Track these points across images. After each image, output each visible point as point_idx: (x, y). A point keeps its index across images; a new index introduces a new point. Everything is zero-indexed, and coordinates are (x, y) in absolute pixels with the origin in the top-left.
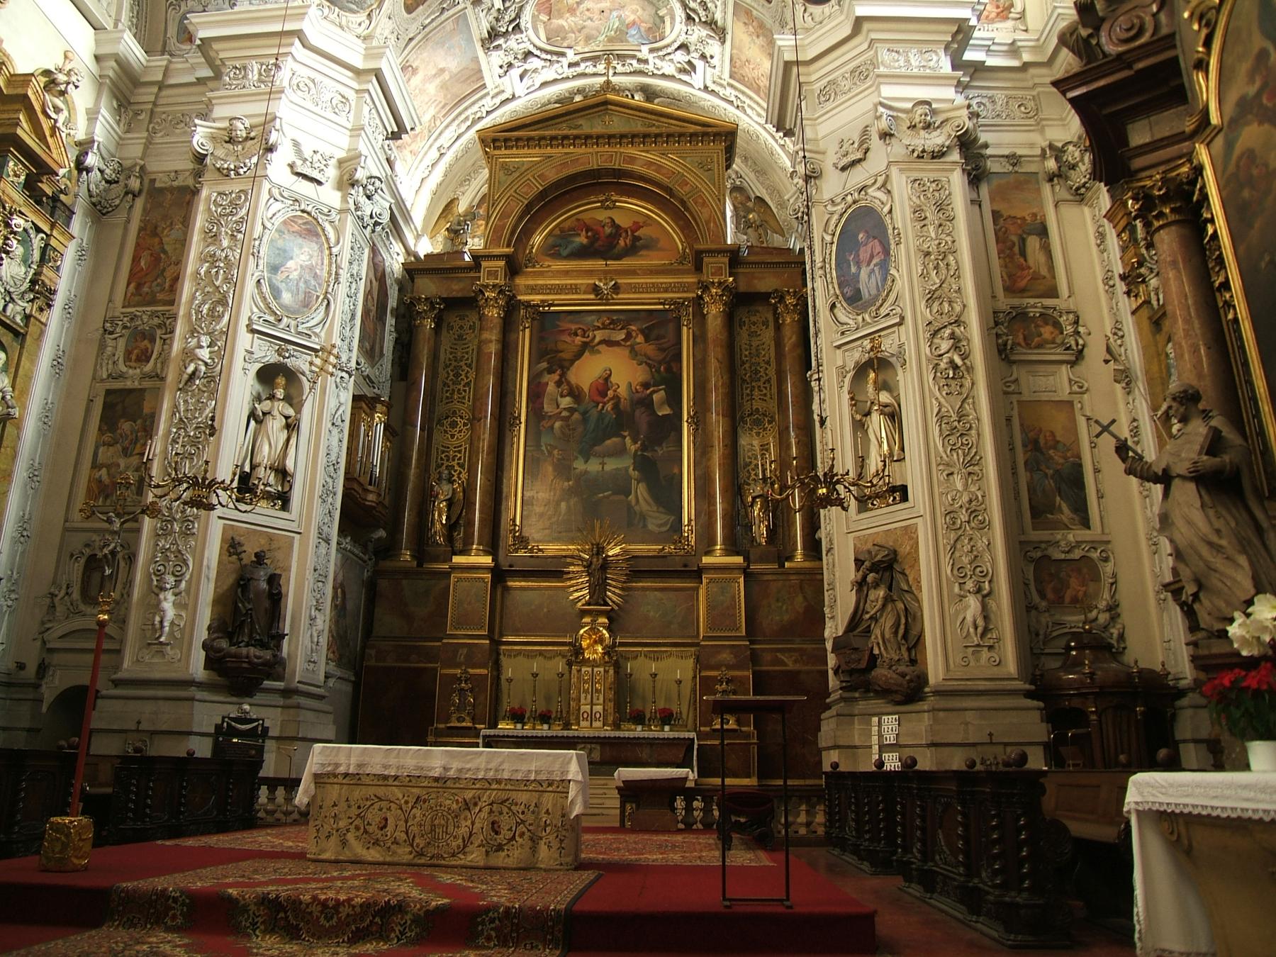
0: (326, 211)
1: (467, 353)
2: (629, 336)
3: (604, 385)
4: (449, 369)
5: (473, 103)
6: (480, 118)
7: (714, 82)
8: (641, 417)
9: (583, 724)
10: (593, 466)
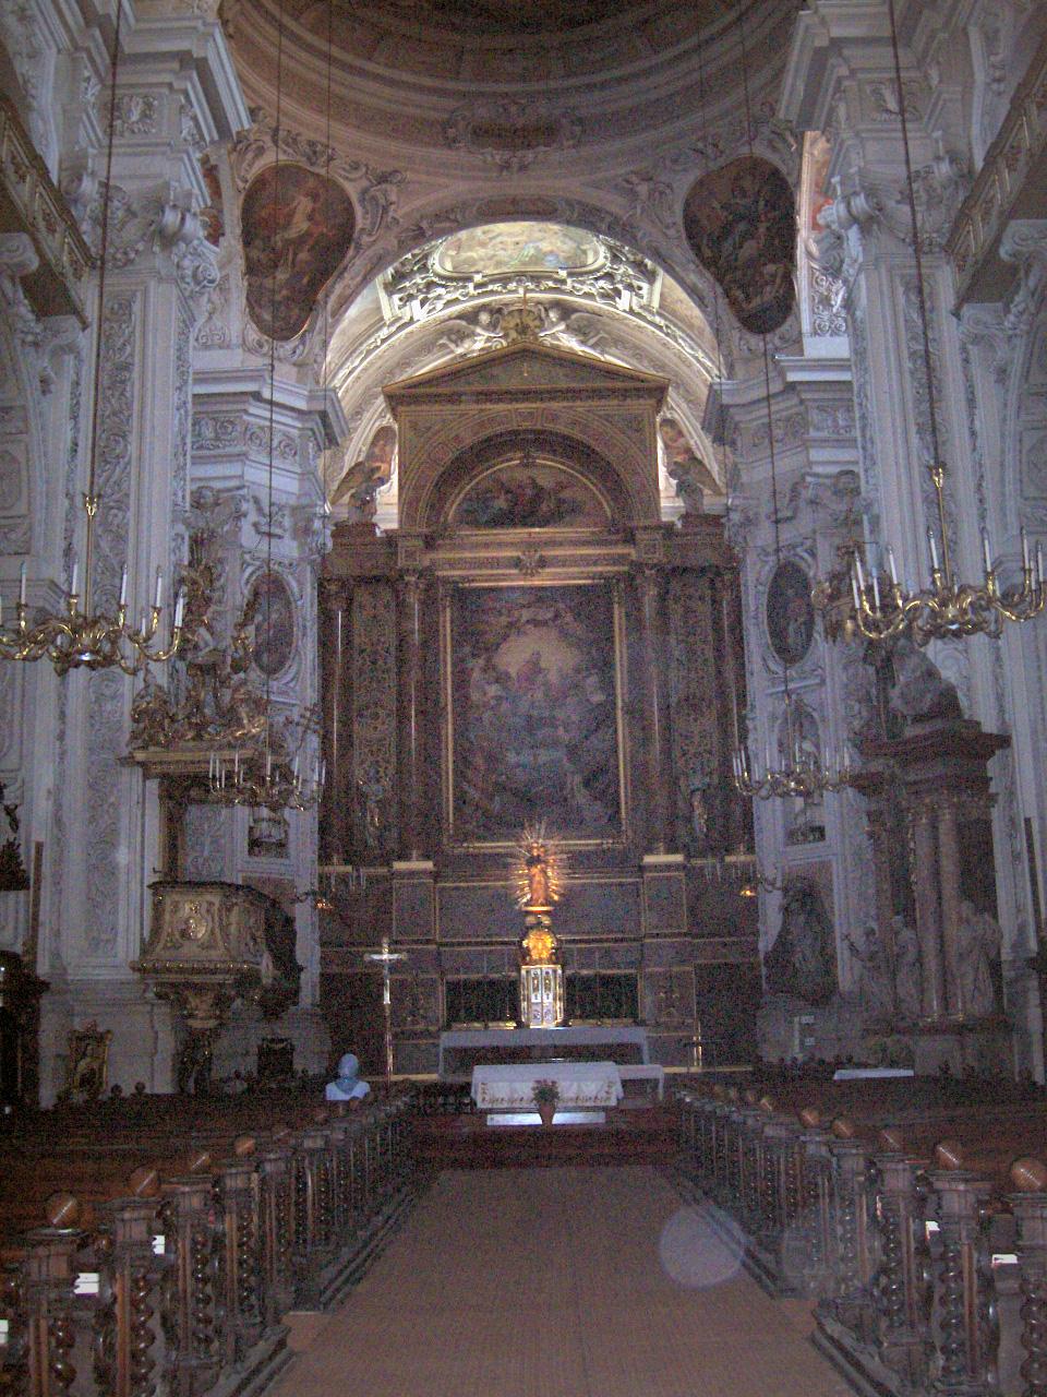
2: (557, 616)
3: (534, 668)
4: (365, 654)
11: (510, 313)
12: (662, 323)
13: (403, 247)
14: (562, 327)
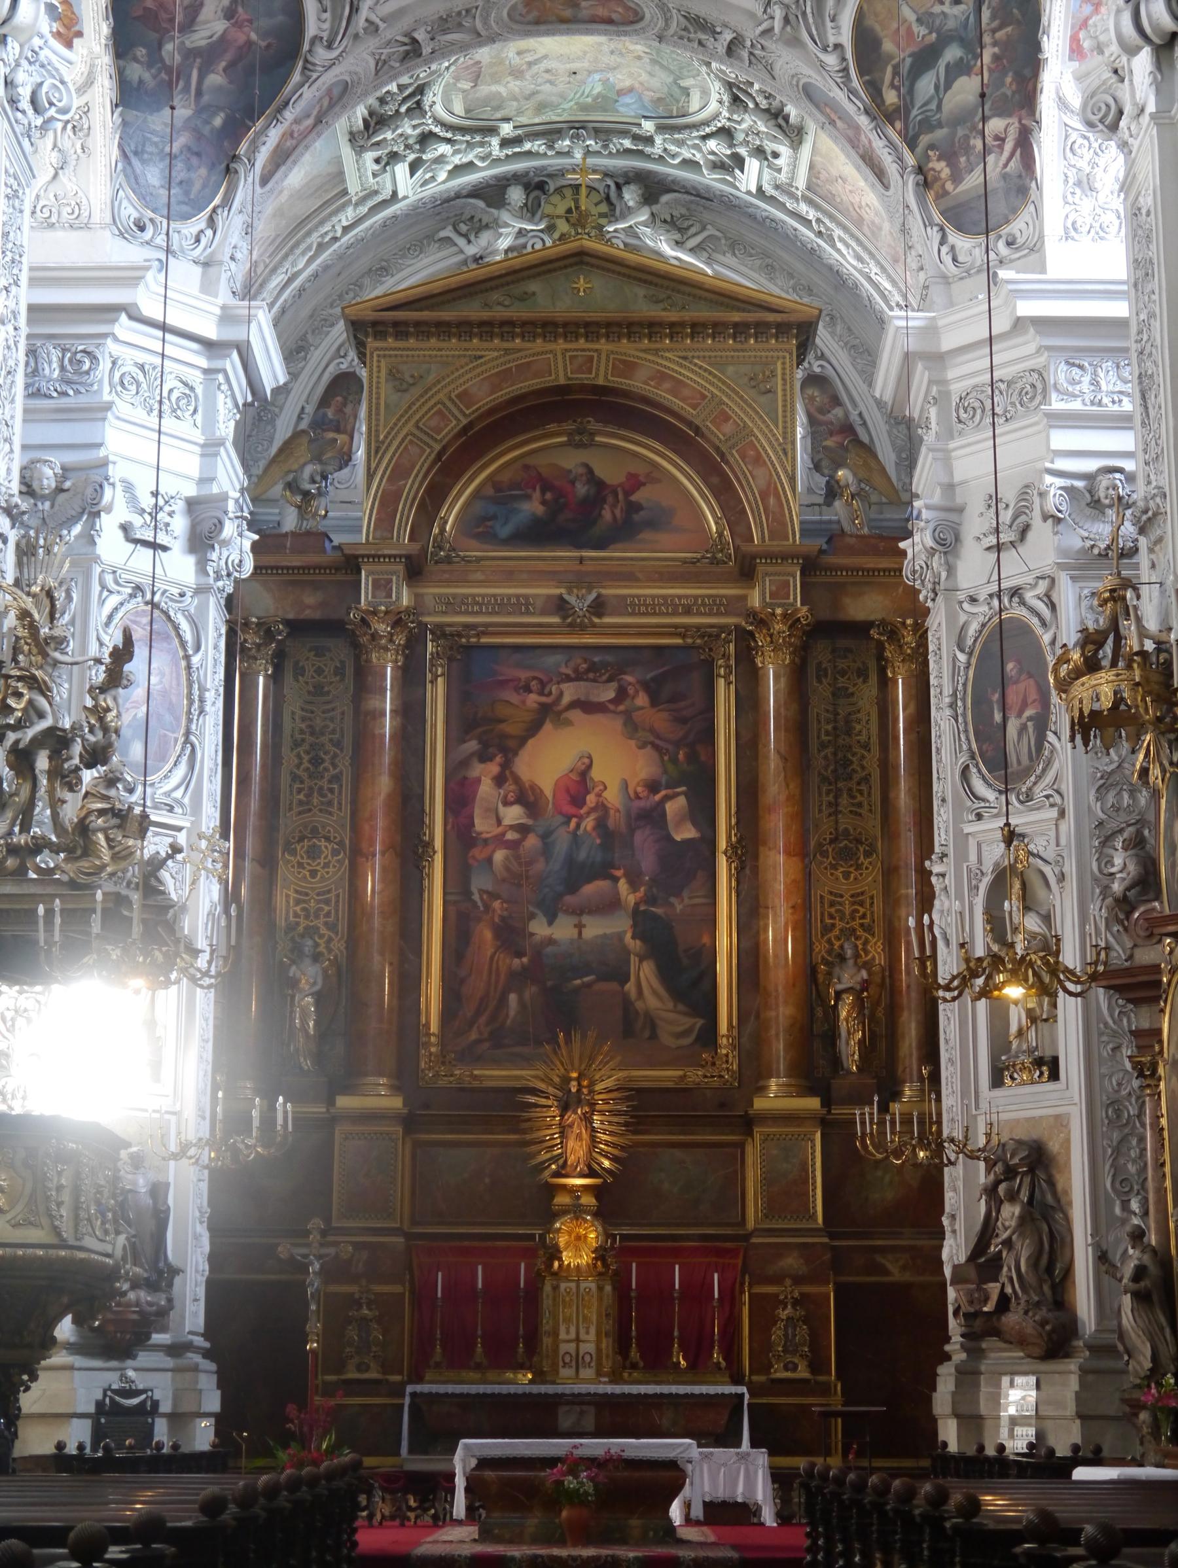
1: (332, 719)
2: (622, 694)
4: (301, 750)
10: (562, 931)
11: (559, 190)
12: (812, 215)
13: (382, 68)
14: (643, 216)
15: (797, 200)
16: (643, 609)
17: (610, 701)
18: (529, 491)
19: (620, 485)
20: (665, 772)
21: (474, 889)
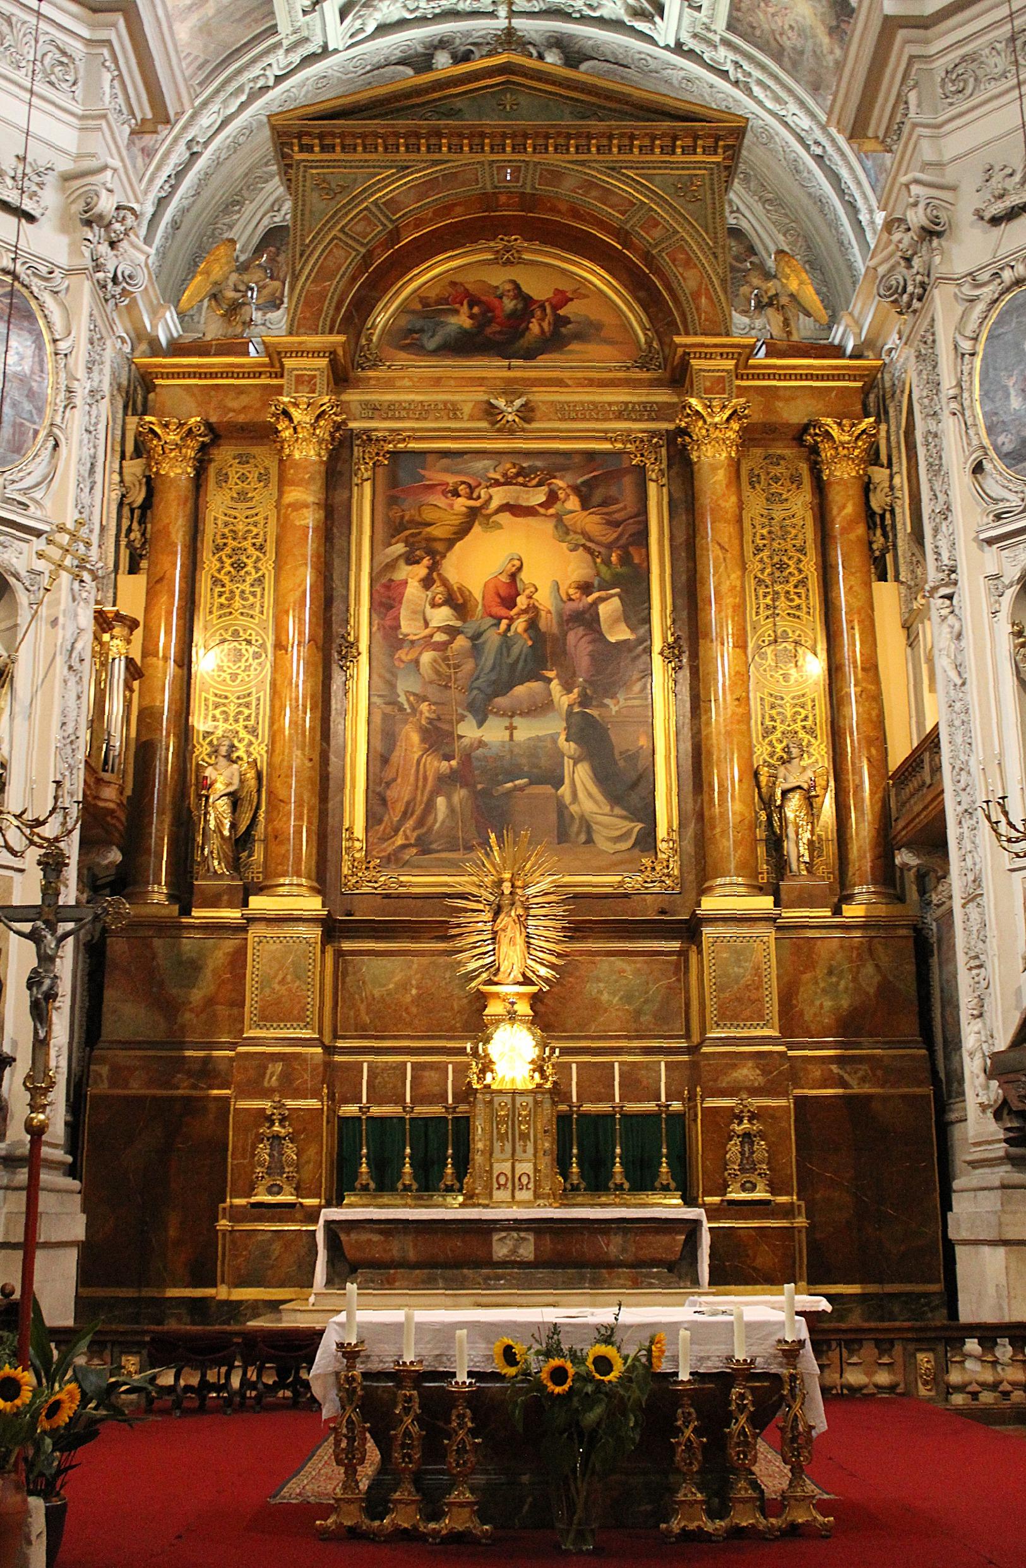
0: (44, 270)
1: (255, 525)
2: (552, 498)
5: (254, 61)
6: (266, 89)
7: (695, 36)
8: (578, 643)
9: (498, 1195)
10: (493, 733)
15: (715, 47)
16: (573, 415)
17: (540, 505)
18: (457, 306)
19: (547, 300)
20: (598, 575)
21: (400, 691)
